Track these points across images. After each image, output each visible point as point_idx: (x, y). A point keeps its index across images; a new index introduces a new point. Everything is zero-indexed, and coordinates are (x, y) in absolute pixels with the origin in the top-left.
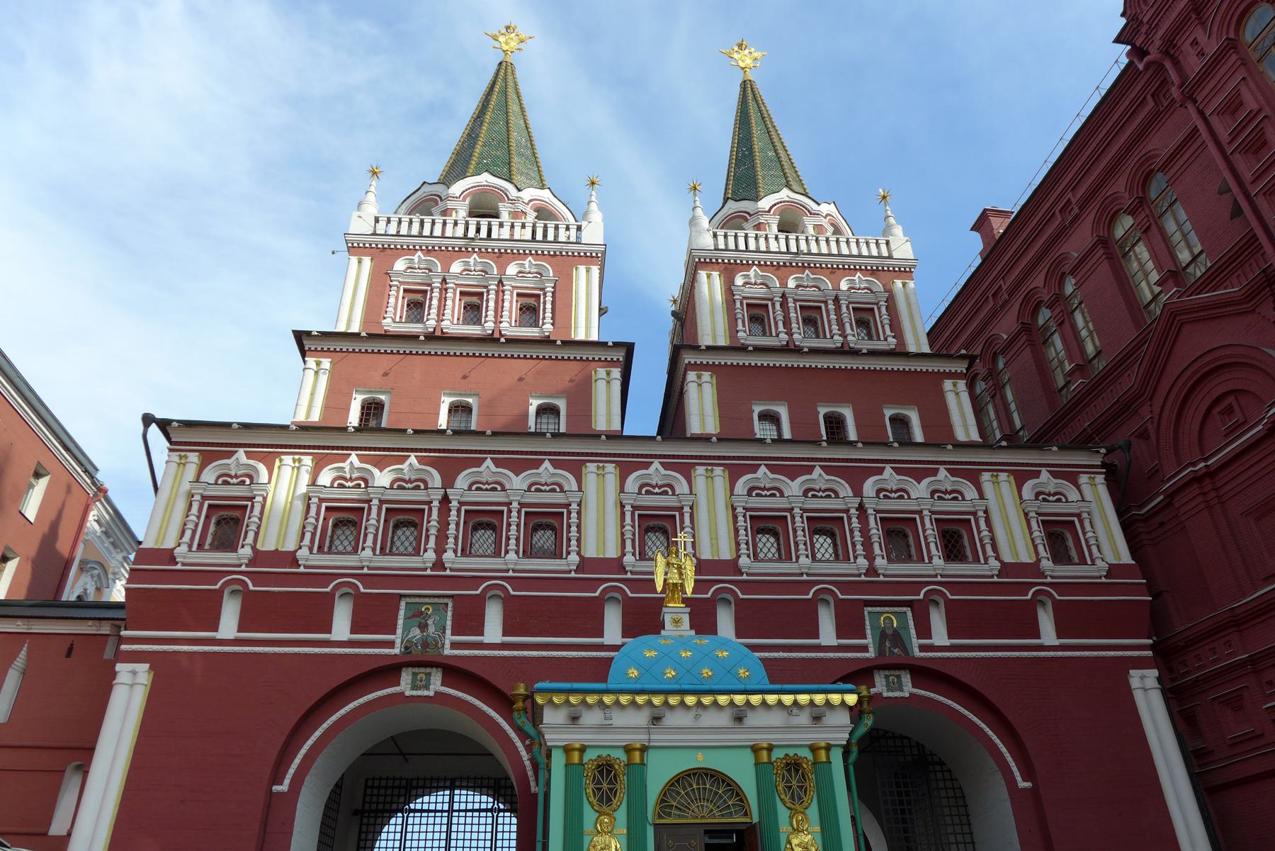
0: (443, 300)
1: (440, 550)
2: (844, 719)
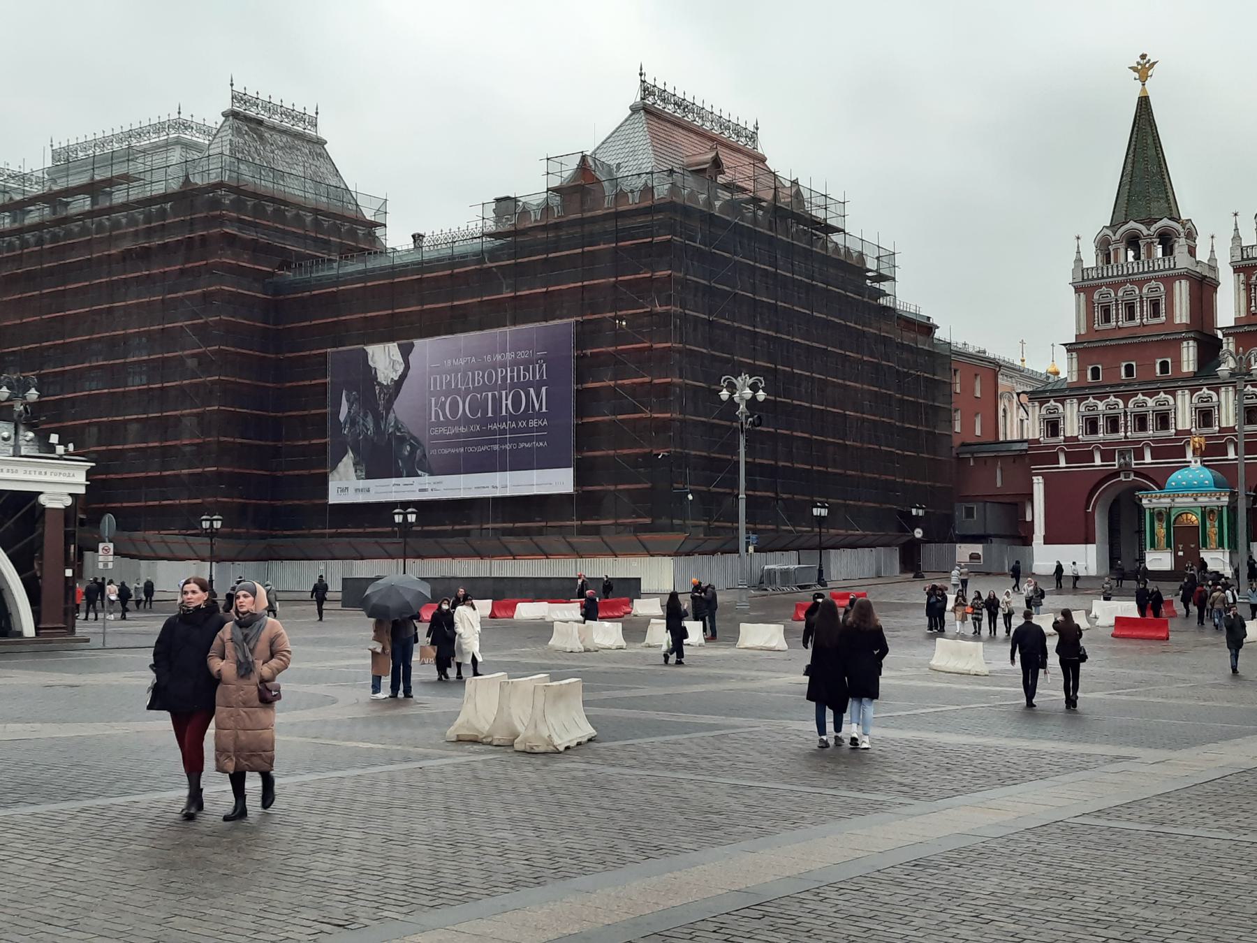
0: (1117, 310)
1: (1126, 432)
2: (1226, 499)
